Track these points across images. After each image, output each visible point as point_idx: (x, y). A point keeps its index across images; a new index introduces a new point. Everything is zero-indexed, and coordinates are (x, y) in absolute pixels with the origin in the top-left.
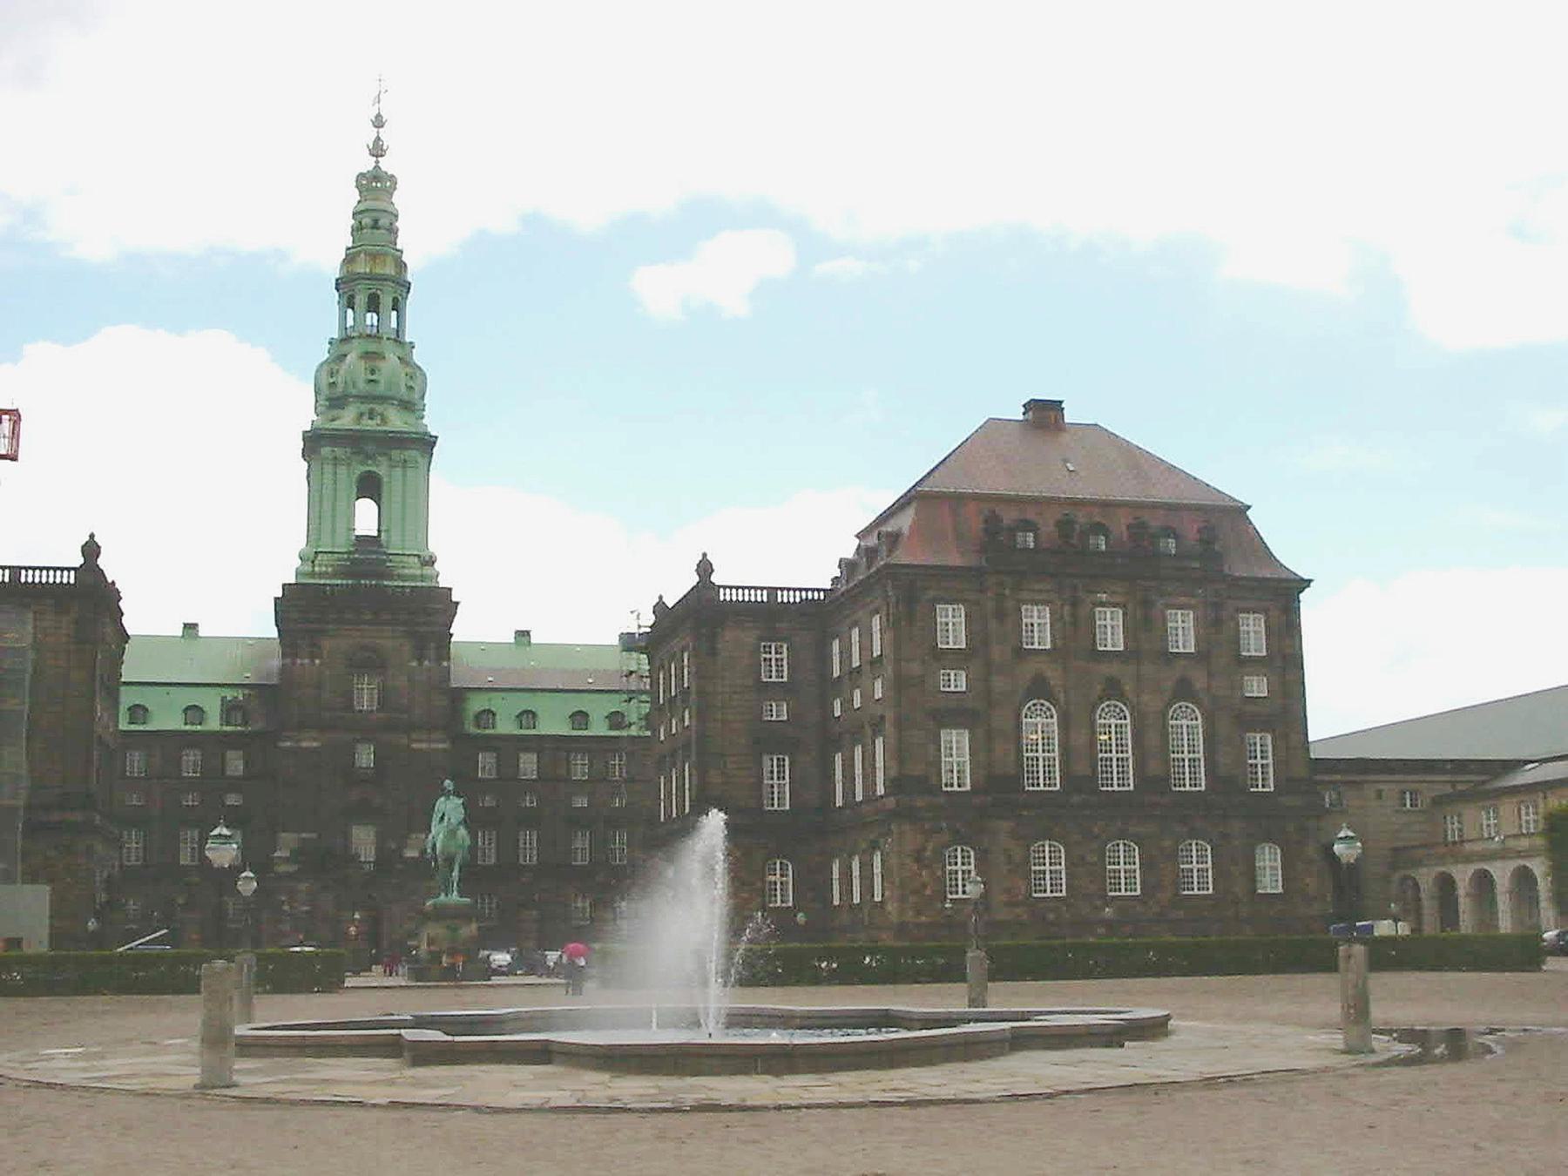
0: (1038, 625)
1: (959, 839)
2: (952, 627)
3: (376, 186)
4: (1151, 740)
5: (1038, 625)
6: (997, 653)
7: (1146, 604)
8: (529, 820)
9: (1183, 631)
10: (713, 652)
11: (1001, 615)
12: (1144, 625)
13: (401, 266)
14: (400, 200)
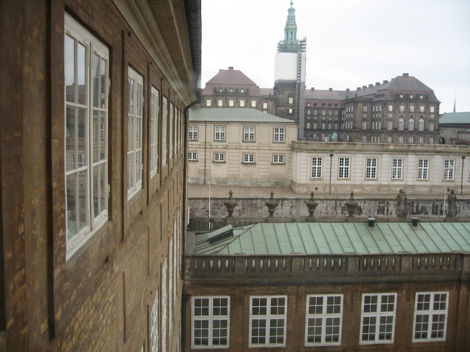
0: (402, 108)
1: (390, 136)
2: (391, 108)
3: (291, 11)
5: (402, 108)
6: (397, 112)
7: (417, 105)
8: (315, 121)
10: (357, 107)
11: (397, 107)
12: (417, 108)
13: (296, 26)
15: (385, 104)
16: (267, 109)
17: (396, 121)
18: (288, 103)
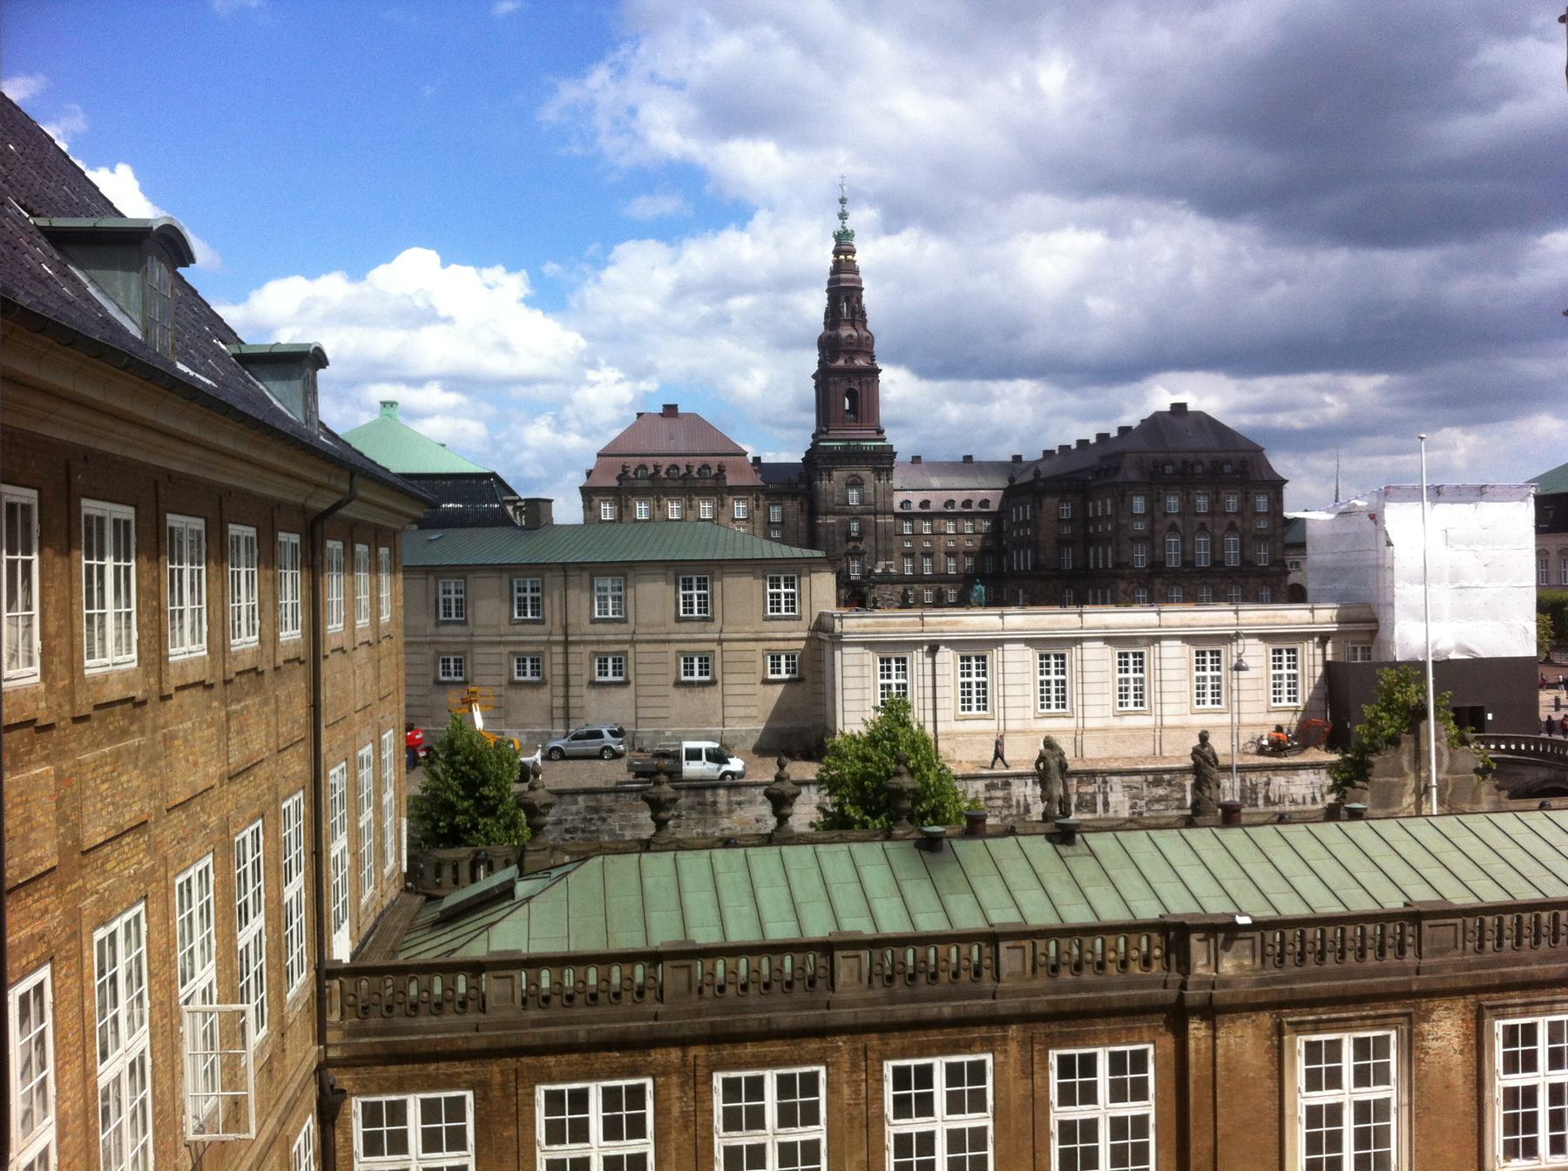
1: (1141, 586)
2: (1139, 505)
4: (1216, 547)
6: (1158, 515)
7: (1217, 493)
9: (1232, 503)
12: (1215, 501)
14: (856, 243)
15: (1123, 495)
16: (782, 523)
17: (1158, 540)
18: (847, 503)
